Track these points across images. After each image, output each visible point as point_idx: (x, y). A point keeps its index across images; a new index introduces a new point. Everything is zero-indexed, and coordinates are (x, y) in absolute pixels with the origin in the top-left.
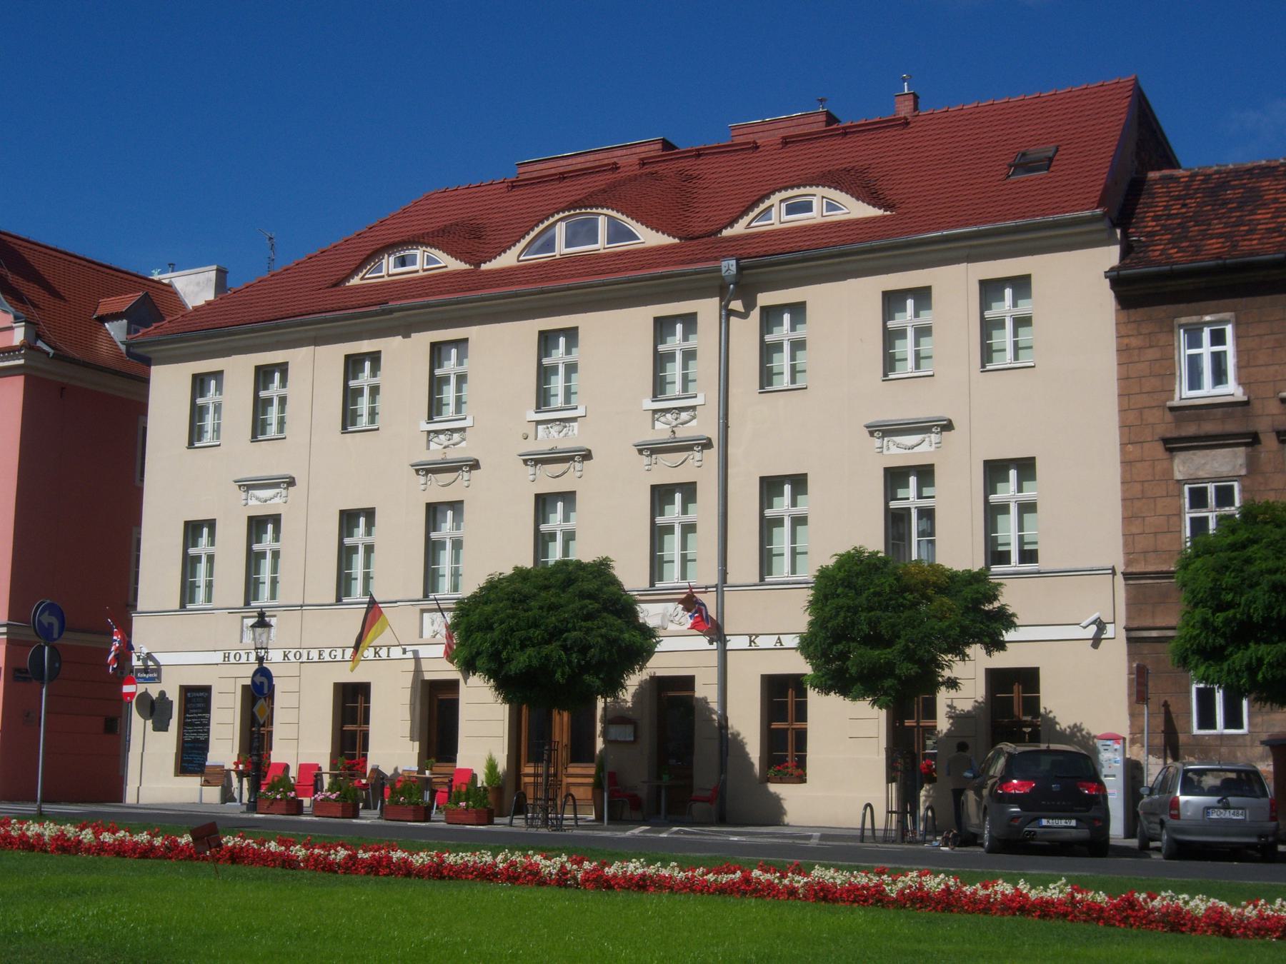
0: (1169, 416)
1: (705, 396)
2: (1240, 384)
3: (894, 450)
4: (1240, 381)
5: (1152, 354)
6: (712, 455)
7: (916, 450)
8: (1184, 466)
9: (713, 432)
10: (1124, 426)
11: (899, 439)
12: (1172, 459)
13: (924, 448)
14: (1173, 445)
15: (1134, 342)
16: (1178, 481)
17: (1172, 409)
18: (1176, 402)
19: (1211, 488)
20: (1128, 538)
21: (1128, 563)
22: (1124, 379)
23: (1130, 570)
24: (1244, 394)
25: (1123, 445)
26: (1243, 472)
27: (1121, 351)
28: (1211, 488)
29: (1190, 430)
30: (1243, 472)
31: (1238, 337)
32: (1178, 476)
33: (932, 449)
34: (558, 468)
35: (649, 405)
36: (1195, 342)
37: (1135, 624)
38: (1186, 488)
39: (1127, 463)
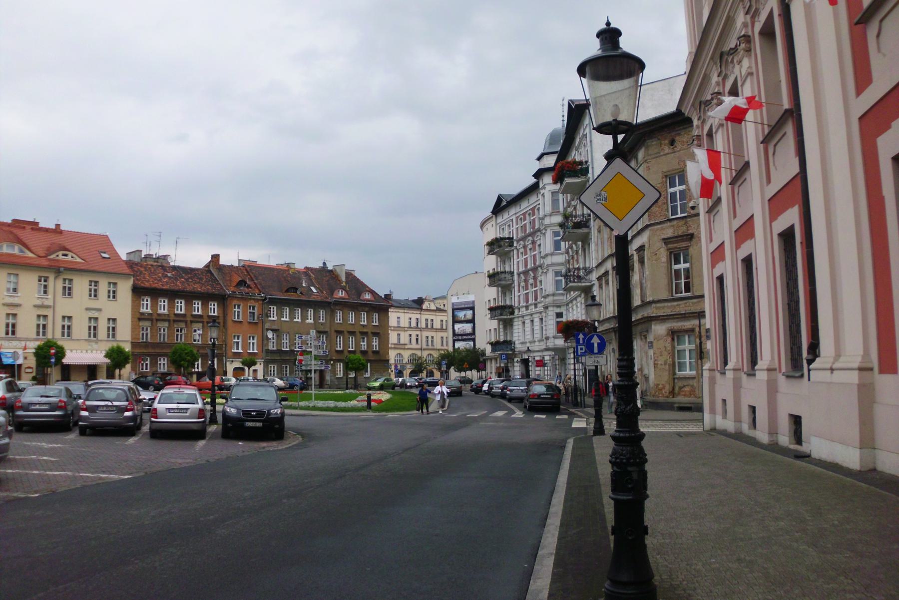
3: (90, 314)
4: (152, 309)
5: (137, 302)
6: (52, 309)
8: (141, 324)
10: (132, 315)
11: (91, 311)
14: (140, 319)
15: (135, 299)
17: (140, 313)
19: (145, 328)
20: (132, 335)
21: (132, 340)
22: (132, 306)
23: (133, 341)
26: (150, 325)
27: (132, 300)
28: (145, 328)
29: (143, 317)
30: (150, 325)
31: (151, 301)
34: (12, 308)
35: (36, 295)
36: (143, 300)
37: (133, 351)
38: (141, 327)
39: (132, 322)
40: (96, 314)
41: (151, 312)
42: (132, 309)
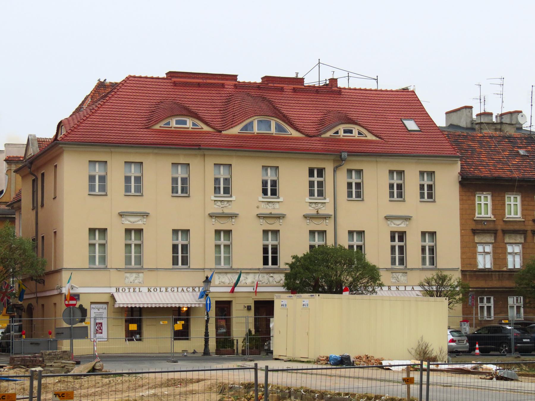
0: (474, 223)
1: (329, 199)
2: (493, 215)
3: (393, 225)
7: (400, 226)
9: (332, 213)
12: (474, 235)
13: (402, 225)
14: (475, 232)
16: (476, 243)
18: (475, 219)
24: (494, 218)
25: (461, 230)
26: (493, 242)
29: (479, 227)
30: (493, 242)
31: (493, 200)
32: (476, 241)
33: (405, 226)
40: (401, 226)
41: (493, 218)
42: (461, 215)
